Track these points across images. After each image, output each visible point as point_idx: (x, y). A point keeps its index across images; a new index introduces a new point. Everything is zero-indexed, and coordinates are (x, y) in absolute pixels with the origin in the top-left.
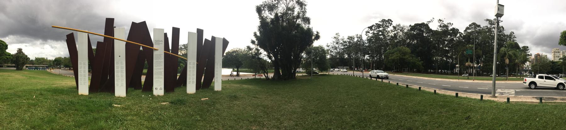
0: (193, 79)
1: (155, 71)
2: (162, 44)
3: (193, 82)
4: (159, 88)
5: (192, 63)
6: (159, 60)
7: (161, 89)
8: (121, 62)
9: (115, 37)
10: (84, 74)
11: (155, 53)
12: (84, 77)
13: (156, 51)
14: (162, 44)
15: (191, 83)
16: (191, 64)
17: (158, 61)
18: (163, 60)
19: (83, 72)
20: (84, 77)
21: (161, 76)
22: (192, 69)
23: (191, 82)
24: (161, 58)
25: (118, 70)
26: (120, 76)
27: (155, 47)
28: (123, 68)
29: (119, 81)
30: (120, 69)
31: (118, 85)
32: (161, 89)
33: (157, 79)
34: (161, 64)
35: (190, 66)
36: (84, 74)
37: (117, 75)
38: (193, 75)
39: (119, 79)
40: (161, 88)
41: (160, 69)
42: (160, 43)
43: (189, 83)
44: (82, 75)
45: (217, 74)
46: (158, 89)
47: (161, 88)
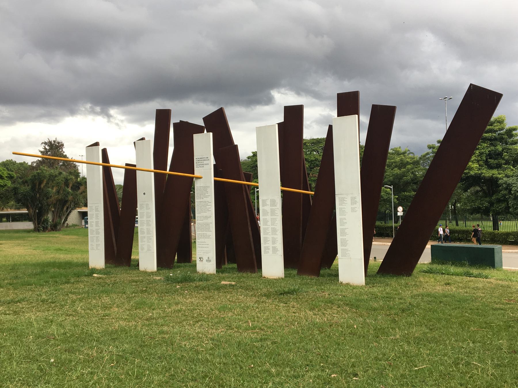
0: (274, 242)
4: (205, 258)
5: (268, 202)
7: (209, 260)
10: (97, 228)
11: (198, 185)
12: (96, 234)
13: (199, 180)
15: (271, 251)
16: (266, 205)
17: (201, 200)
19: (94, 224)
20: (96, 234)
22: (269, 217)
24: (207, 195)
26: (145, 231)
29: (144, 242)
30: (145, 219)
32: (209, 260)
34: (207, 207)
35: (265, 208)
36: (97, 228)
37: (142, 229)
38: (274, 231)
39: (144, 237)
41: (206, 218)
42: (205, 162)
43: (266, 252)
45: (343, 230)
46: (204, 260)
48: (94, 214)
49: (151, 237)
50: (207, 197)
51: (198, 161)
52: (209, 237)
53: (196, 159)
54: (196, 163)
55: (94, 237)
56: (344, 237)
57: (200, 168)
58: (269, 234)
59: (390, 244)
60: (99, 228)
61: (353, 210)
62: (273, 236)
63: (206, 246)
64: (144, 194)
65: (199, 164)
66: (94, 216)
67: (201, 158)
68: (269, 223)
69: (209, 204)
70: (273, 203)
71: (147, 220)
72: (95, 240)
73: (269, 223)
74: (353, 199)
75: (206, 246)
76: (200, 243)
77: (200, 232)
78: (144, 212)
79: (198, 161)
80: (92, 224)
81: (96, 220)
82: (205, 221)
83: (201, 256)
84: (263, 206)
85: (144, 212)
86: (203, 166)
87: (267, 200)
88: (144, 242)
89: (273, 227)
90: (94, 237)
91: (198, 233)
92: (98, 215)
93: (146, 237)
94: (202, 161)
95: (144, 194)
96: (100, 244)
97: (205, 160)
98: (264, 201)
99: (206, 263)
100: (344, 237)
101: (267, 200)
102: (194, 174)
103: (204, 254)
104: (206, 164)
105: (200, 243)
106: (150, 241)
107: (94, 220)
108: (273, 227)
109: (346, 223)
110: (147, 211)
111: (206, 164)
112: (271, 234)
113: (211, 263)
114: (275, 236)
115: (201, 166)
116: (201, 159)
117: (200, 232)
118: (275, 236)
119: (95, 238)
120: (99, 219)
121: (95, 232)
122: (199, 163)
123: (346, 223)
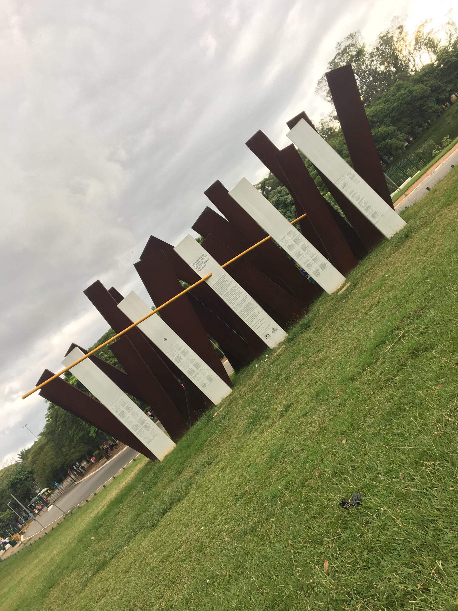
1: (239, 310)
2: (208, 259)
3: (323, 266)
4: (270, 332)
5: (288, 238)
6: (229, 288)
7: (274, 330)
8: (177, 346)
9: (135, 323)
11: (211, 284)
12: (142, 424)
13: (210, 279)
14: (208, 259)
15: (321, 271)
16: (287, 241)
17: (227, 292)
18: (234, 283)
19: (132, 419)
20: (142, 424)
21: (255, 311)
22: (297, 248)
23: (318, 270)
24: (228, 283)
25: (182, 362)
26: (194, 368)
27: (203, 275)
28: (188, 353)
29: (201, 377)
30: (184, 359)
31: (204, 385)
32: (274, 330)
33: (255, 321)
34: (237, 292)
35: (288, 244)
38: (310, 253)
39: (198, 374)
40: (273, 329)
41: (244, 300)
42: (204, 260)
44: (137, 424)
46: (271, 334)
47: (273, 329)
48: (125, 410)
49: (204, 368)
50: (230, 284)
51: (197, 265)
52: (259, 313)
53: (193, 265)
54: (196, 268)
55: (142, 428)
56: (366, 206)
57: (203, 269)
58: (308, 259)
59: (227, 360)
60: (140, 416)
61: (356, 182)
62: (312, 258)
63: (262, 322)
64: (165, 340)
65: (199, 267)
66: (125, 411)
67: (197, 261)
68: (302, 252)
69: (236, 288)
70: (291, 234)
71: (187, 359)
72: (145, 431)
73: (302, 252)
74: (350, 175)
75: (262, 322)
76: (256, 325)
77: (248, 317)
78: (179, 355)
79: (197, 265)
80: (129, 420)
81: (131, 413)
82: (244, 305)
83: (265, 335)
84: (285, 244)
85: (179, 355)
86: (204, 265)
87: (284, 237)
88: (201, 377)
89: (306, 251)
90: (142, 428)
91: (246, 319)
92: (129, 406)
93: (199, 372)
94: (201, 262)
95: (165, 340)
96: (154, 429)
97: (203, 259)
98: (283, 241)
99: (274, 334)
100: (366, 206)
101: (284, 237)
102: (201, 279)
103: (266, 329)
104: (206, 261)
105: (256, 325)
106: (205, 372)
107: (184, 359)
108: (306, 251)
109: (359, 195)
110: (181, 351)
111: (206, 261)
112: (309, 258)
113: (278, 330)
114: (315, 256)
115: (202, 266)
116: (197, 262)
117: (248, 317)
118: (315, 256)
119: (144, 429)
120: (133, 409)
121: (139, 424)
122: (198, 266)
123: (359, 195)
